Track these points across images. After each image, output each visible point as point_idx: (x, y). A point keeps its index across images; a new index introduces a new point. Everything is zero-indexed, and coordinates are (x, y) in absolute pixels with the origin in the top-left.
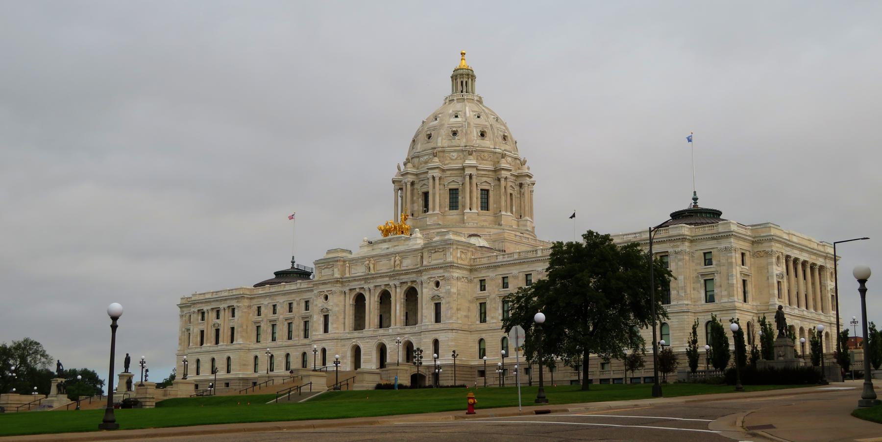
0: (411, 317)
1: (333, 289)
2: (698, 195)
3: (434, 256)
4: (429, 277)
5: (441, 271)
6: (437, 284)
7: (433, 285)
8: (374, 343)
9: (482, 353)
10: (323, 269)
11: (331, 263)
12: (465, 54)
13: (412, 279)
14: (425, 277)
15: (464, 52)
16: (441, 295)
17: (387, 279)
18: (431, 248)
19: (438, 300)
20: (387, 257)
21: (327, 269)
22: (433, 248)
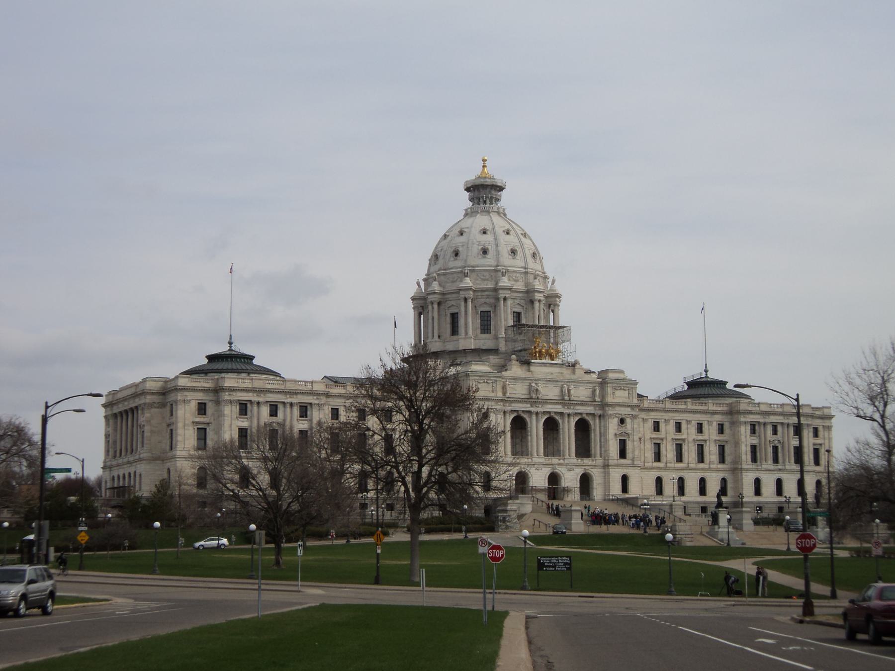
0: (584, 449)
1: (498, 407)
2: (708, 368)
3: (619, 393)
4: (615, 413)
5: (629, 409)
6: (622, 421)
7: (616, 421)
8: (546, 471)
9: (659, 491)
10: (480, 383)
11: (492, 379)
12: (486, 160)
13: (588, 412)
14: (610, 411)
15: (486, 158)
16: (629, 432)
17: (560, 407)
18: (615, 385)
19: (624, 436)
20: (554, 383)
21: (485, 384)
22: (619, 385)
